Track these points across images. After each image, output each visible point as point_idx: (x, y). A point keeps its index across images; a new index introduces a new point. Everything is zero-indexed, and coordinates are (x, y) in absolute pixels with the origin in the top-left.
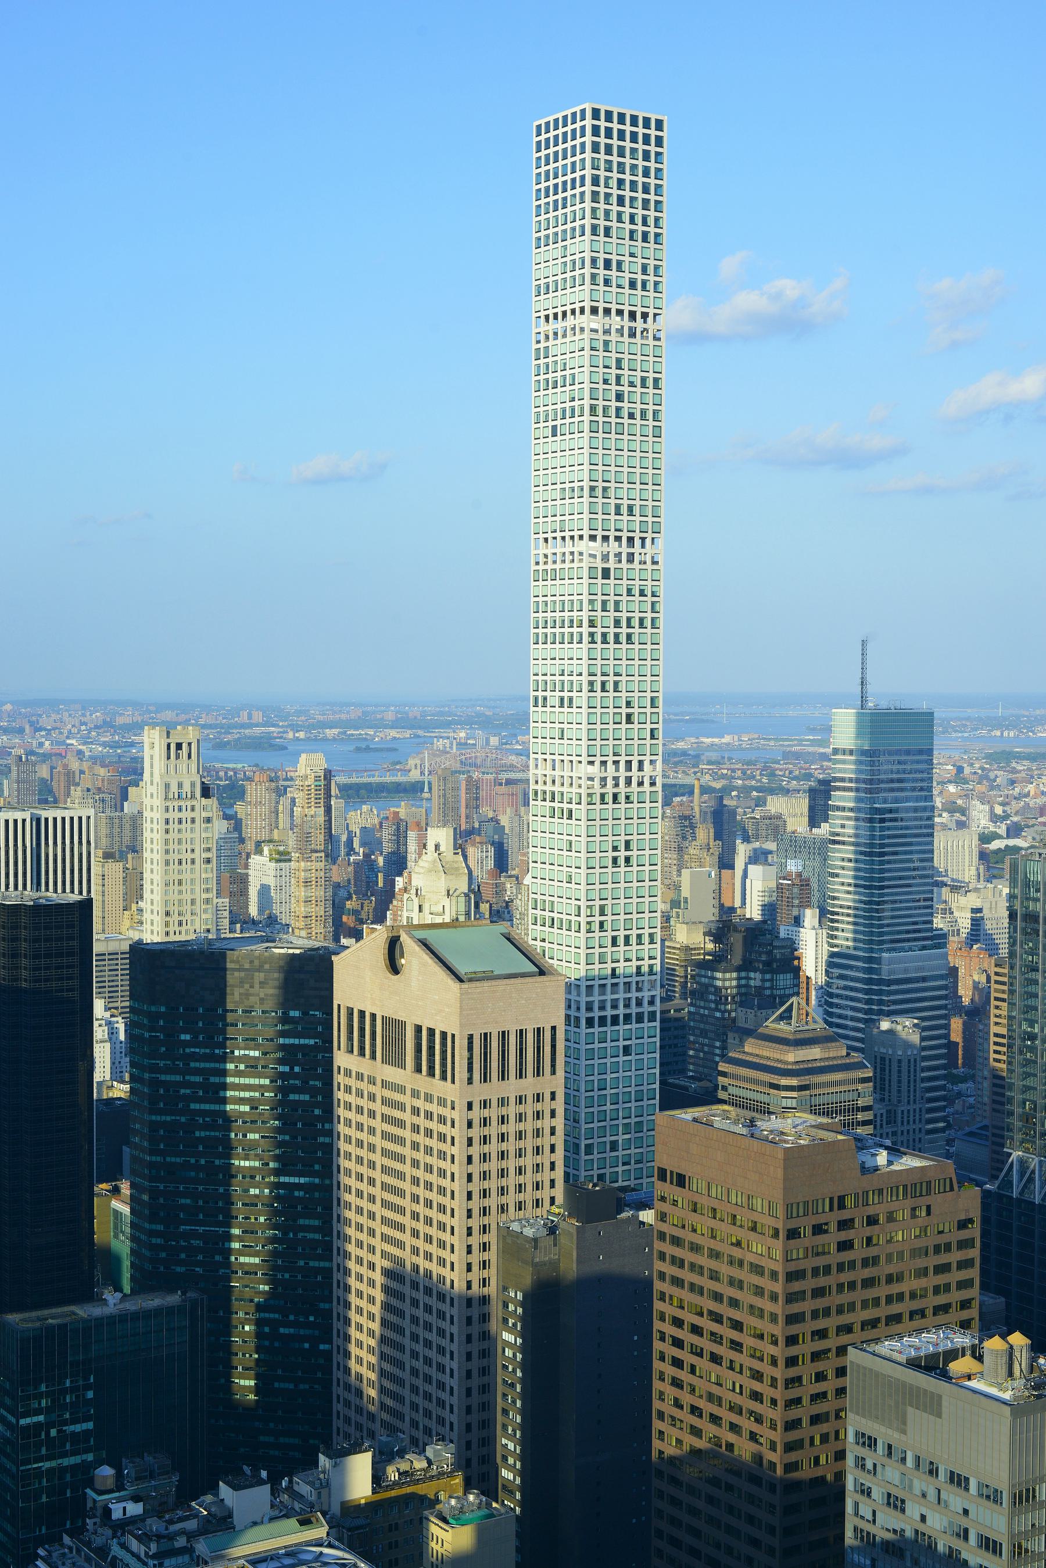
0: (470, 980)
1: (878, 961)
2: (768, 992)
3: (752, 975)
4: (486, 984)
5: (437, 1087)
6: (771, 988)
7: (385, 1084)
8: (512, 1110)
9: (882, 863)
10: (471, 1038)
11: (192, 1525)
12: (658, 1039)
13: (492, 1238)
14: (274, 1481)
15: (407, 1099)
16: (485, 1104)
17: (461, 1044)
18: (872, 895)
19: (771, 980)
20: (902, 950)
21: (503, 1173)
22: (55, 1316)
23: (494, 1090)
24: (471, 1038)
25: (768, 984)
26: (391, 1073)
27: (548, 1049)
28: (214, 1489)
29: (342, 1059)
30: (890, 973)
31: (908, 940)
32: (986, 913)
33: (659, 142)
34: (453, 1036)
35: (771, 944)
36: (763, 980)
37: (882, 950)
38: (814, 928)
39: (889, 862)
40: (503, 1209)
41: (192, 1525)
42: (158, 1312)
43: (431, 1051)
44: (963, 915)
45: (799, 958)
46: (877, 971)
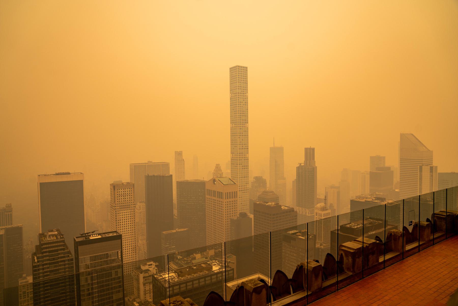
5: (221, 200)
7: (213, 200)
8: (231, 203)
11: (190, 259)
13: (229, 220)
14: (201, 253)
15: (216, 202)
16: (228, 202)
17: (224, 194)
21: (230, 211)
22: (169, 232)
23: (229, 200)
26: (214, 198)
28: (193, 254)
29: (207, 196)
33: (247, 70)
40: (230, 216)
41: (190, 259)
42: (183, 231)
43: (220, 195)
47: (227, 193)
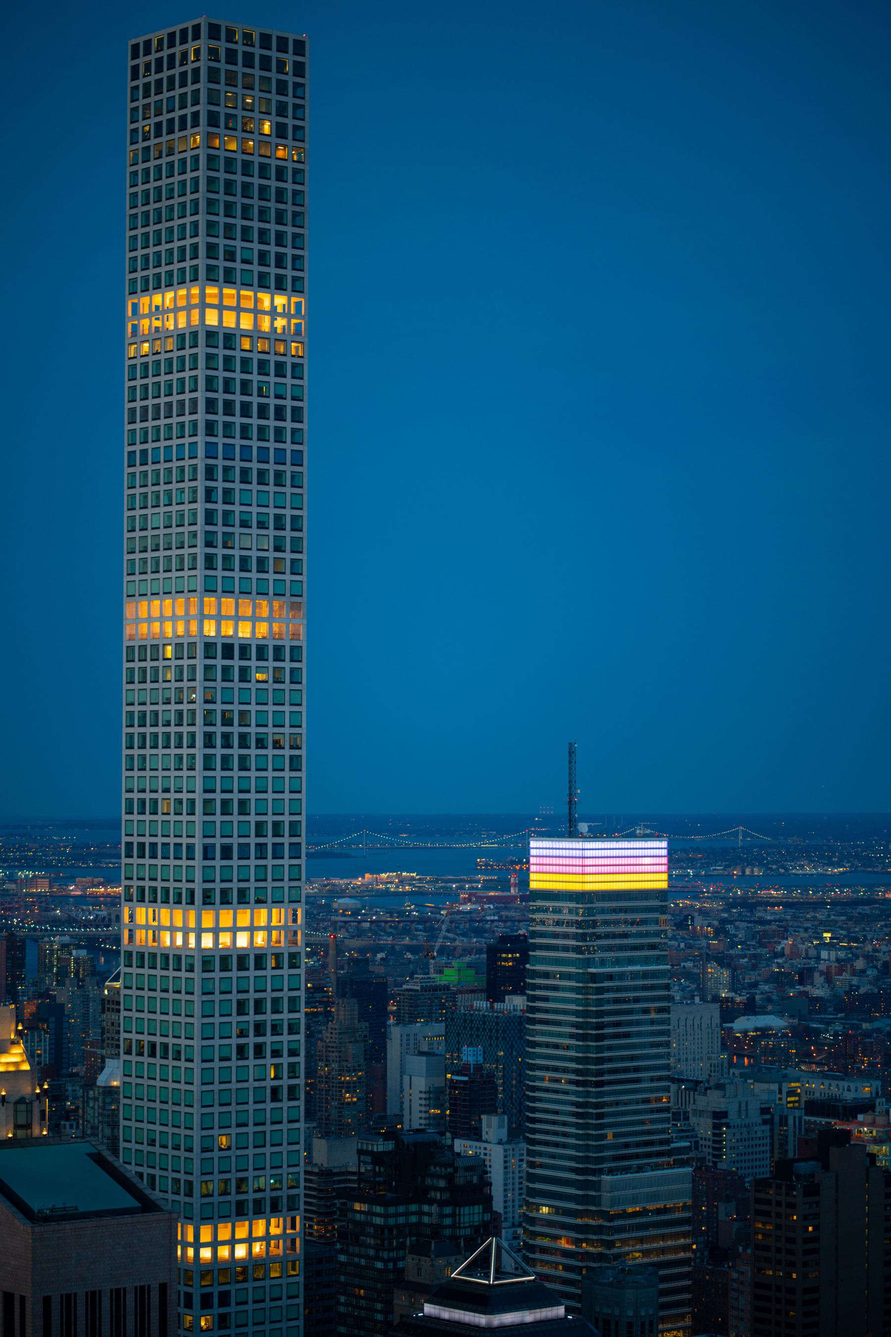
0: (47, 1219)
1: (596, 1186)
2: (448, 1232)
3: (426, 1208)
4: (68, 1226)
6: (453, 1226)
9: (599, 1049)
10: (47, 1301)
12: (300, 1300)
17: (33, 1309)
18: (588, 1094)
19: (453, 1215)
20: (626, 1170)
24: (47, 1301)
25: (448, 1221)
27: (155, 1316)
30: (614, 1202)
31: (637, 1156)
32: (733, 1118)
34: (23, 1299)
35: (452, 1165)
36: (442, 1216)
37: (601, 1171)
38: (500, 1143)
39: (610, 1048)
44: (702, 1120)
45: (490, 1184)
46: (596, 1201)
47: (68, 1300)
